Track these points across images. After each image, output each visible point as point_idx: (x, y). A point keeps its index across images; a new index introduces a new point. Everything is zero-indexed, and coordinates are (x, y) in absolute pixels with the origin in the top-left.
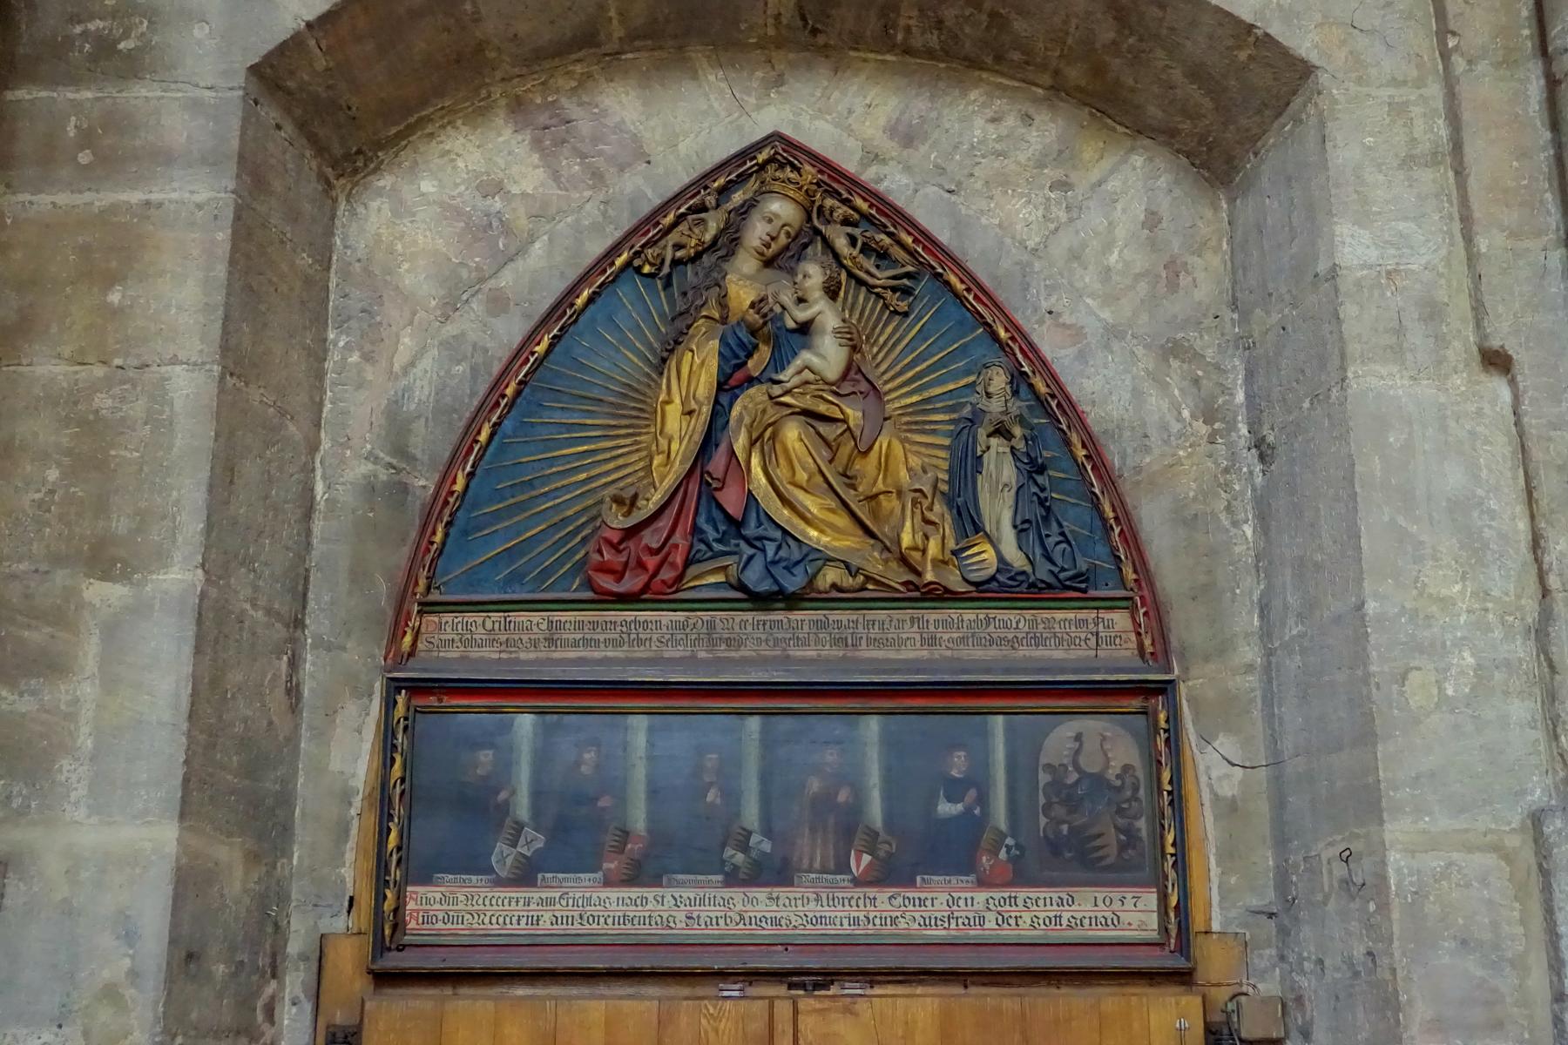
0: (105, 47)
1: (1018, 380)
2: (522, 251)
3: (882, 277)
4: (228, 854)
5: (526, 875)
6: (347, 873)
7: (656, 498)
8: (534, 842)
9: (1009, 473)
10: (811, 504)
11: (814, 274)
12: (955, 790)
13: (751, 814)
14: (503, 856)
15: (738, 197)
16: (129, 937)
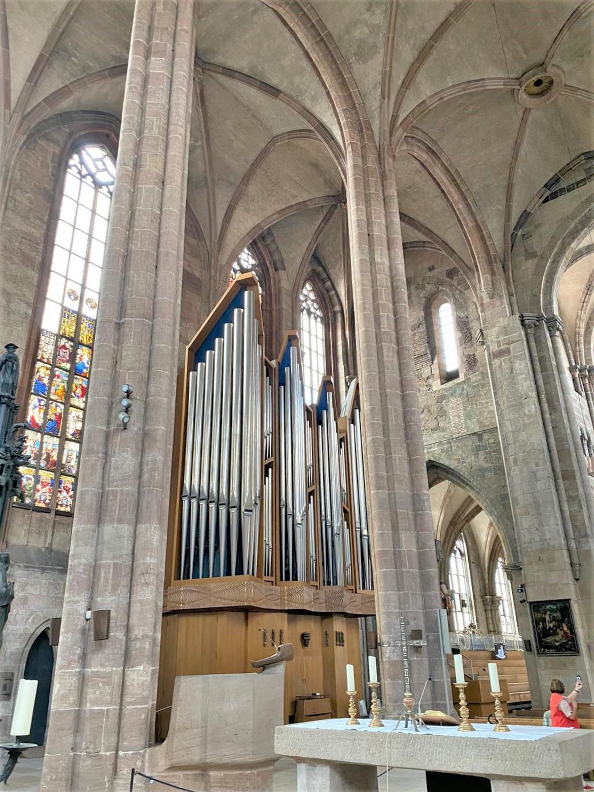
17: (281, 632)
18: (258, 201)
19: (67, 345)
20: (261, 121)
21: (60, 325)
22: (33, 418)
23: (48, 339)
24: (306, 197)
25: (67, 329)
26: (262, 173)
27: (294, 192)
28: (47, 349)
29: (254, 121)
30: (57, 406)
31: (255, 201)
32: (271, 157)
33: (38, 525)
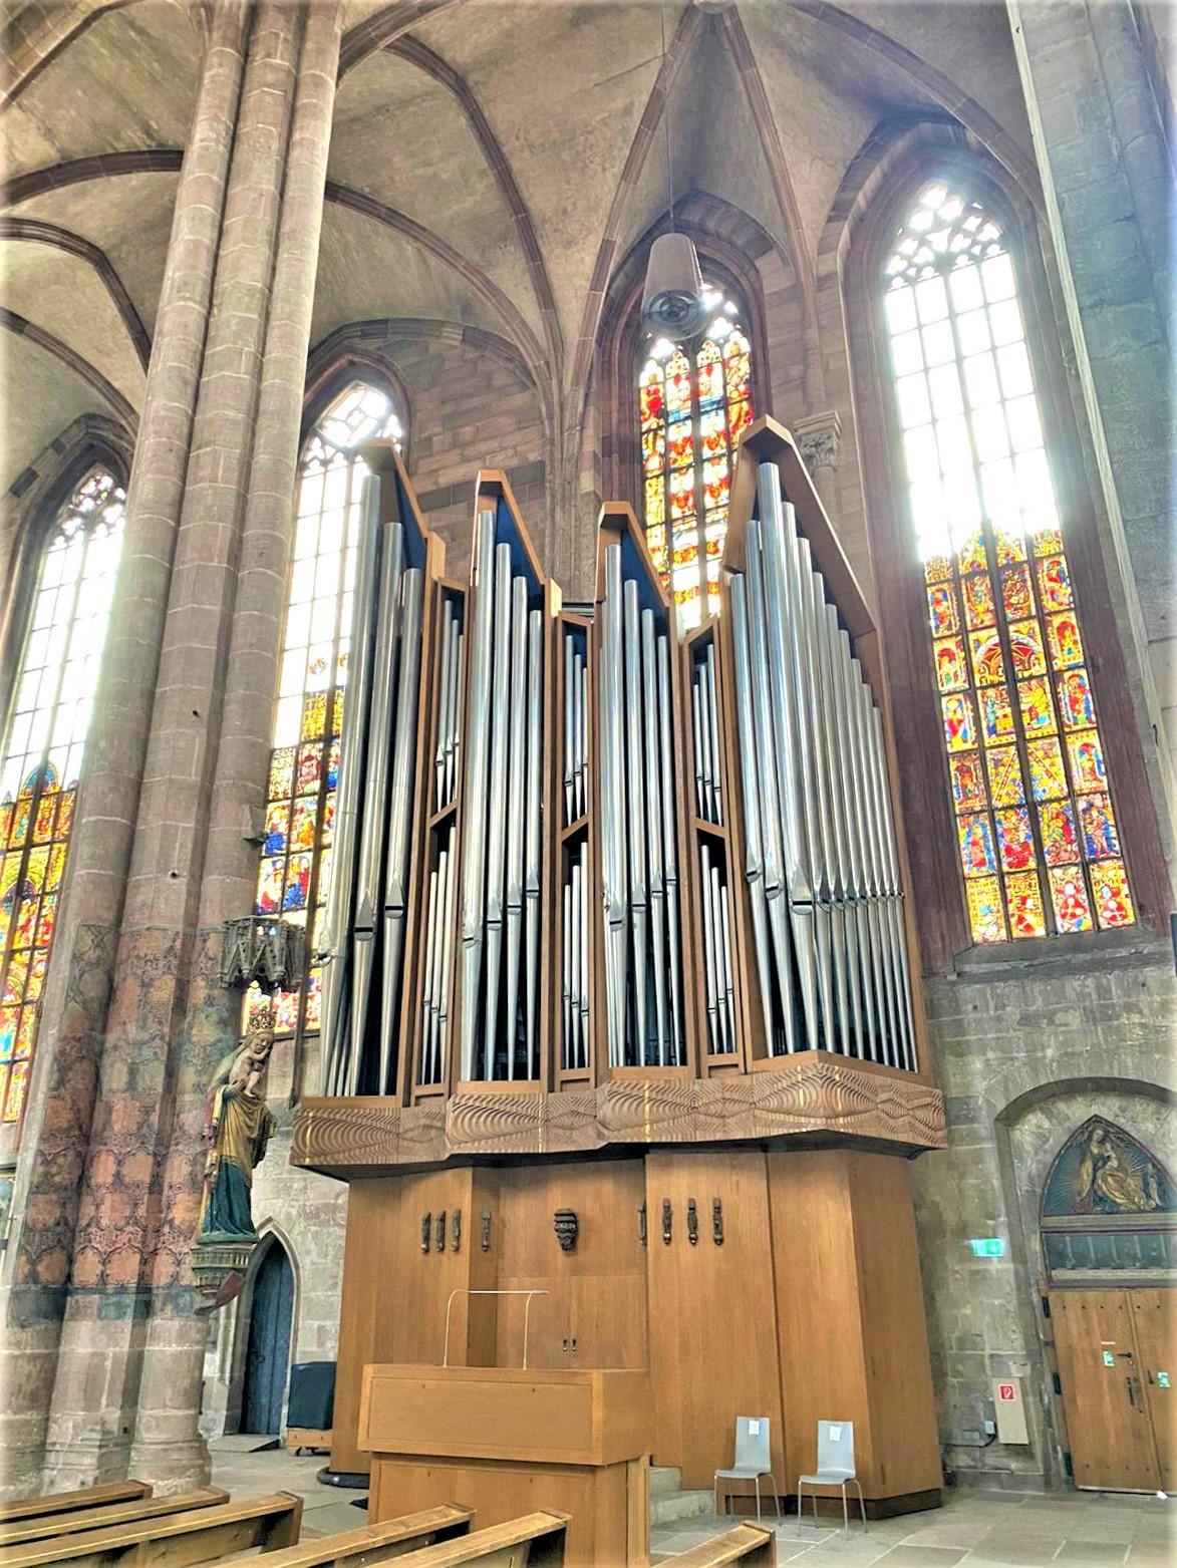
0: (966, 1116)
1: (1154, 1165)
2: (1048, 1140)
3: (1122, 1145)
4: (1020, 1267)
5: (1073, 1268)
6: (1040, 1268)
7: (1084, 1194)
8: (1074, 1262)
9: (1155, 1185)
10: (1116, 1194)
11: (1108, 1146)
12: (1155, 1250)
13: (1115, 1256)
14: (1069, 1265)
15: (1090, 1129)
16: (1009, 1284)
17: (693, 1209)
18: (574, 204)
19: (314, 753)
20: (415, 97)
21: (302, 725)
22: (265, 895)
23: (282, 760)
24: (647, 80)
25: (313, 728)
26: (527, 154)
27: (620, 103)
28: (282, 776)
29: (411, 109)
30: (301, 858)
31: (569, 208)
32: (499, 115)
33: (280, 1063)
